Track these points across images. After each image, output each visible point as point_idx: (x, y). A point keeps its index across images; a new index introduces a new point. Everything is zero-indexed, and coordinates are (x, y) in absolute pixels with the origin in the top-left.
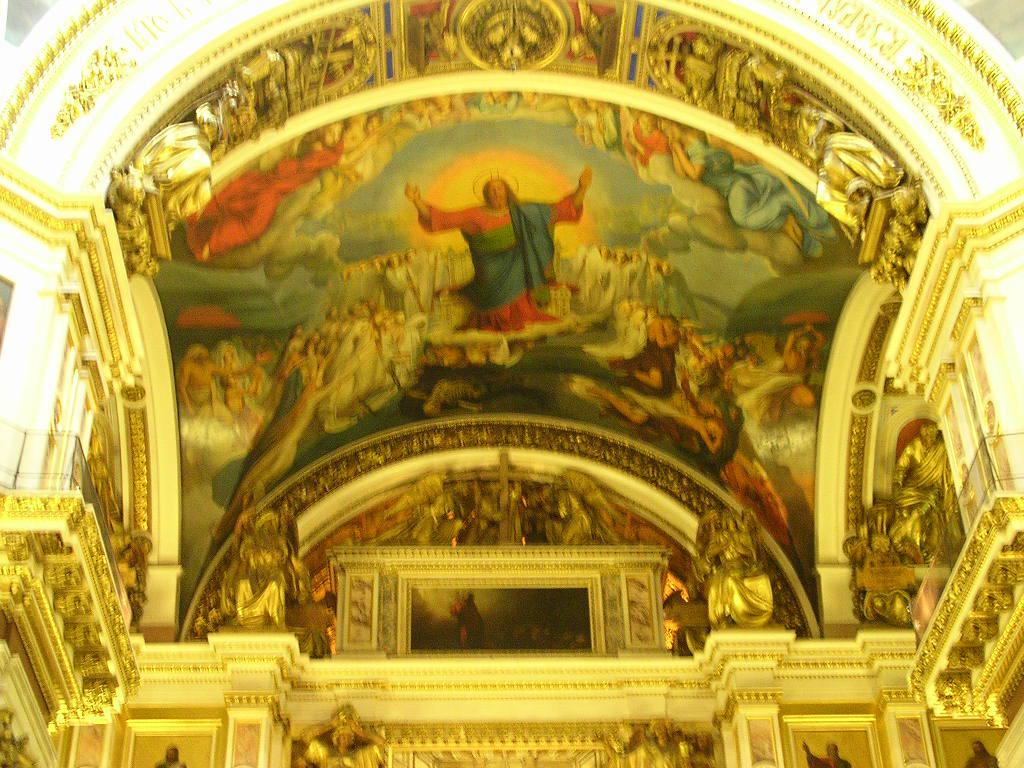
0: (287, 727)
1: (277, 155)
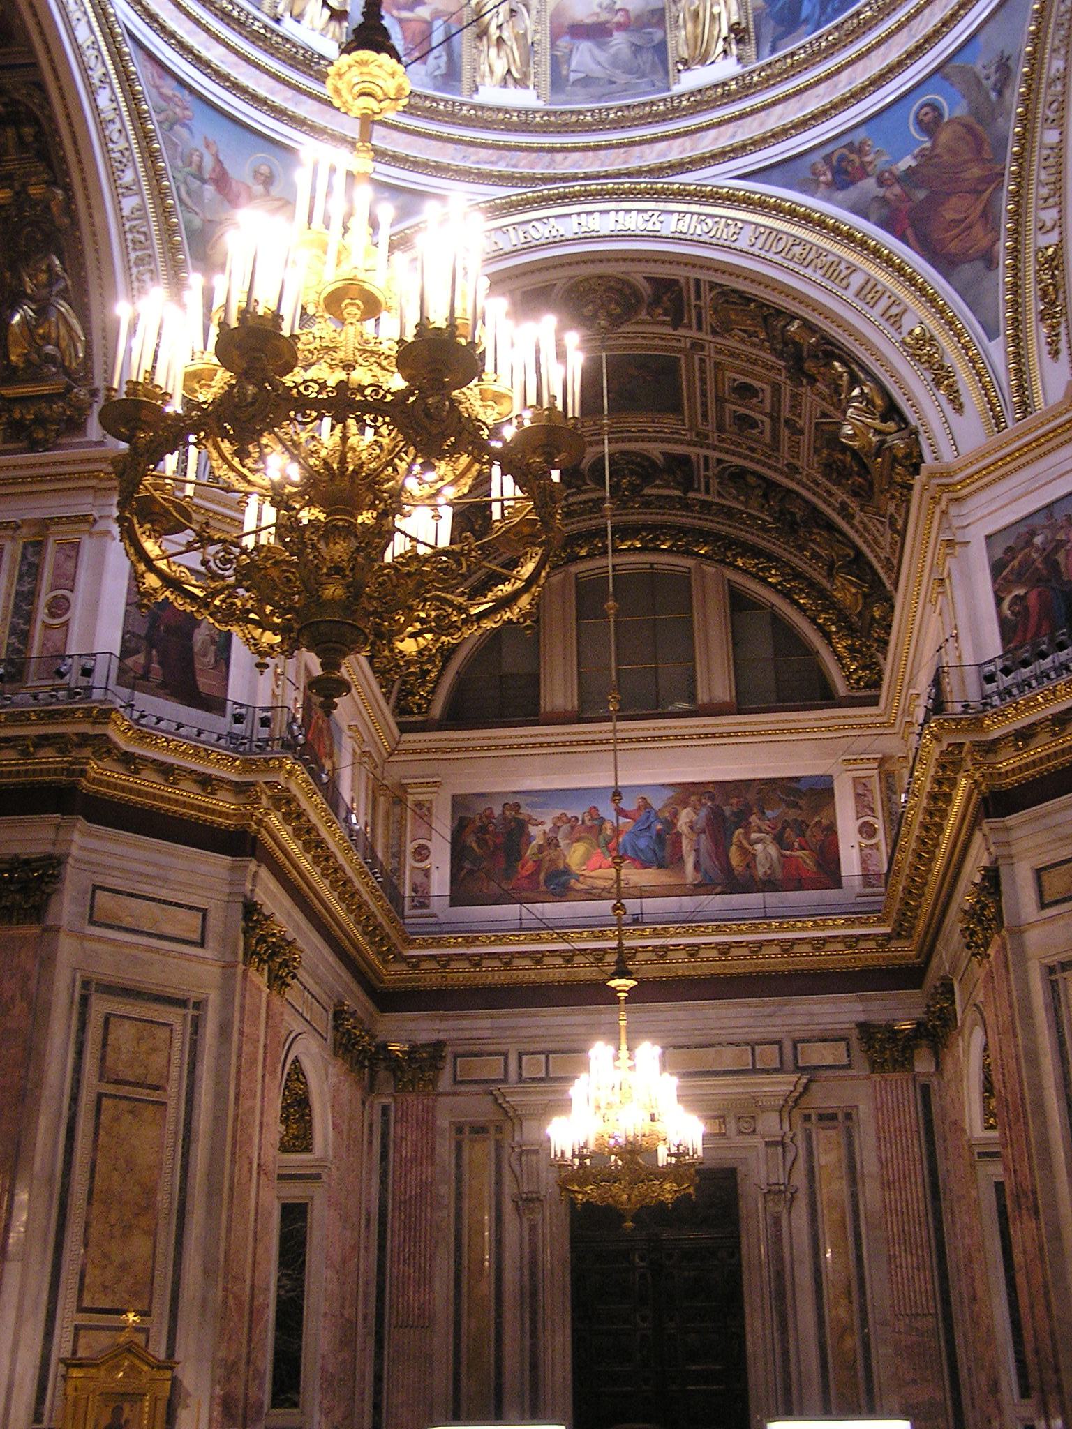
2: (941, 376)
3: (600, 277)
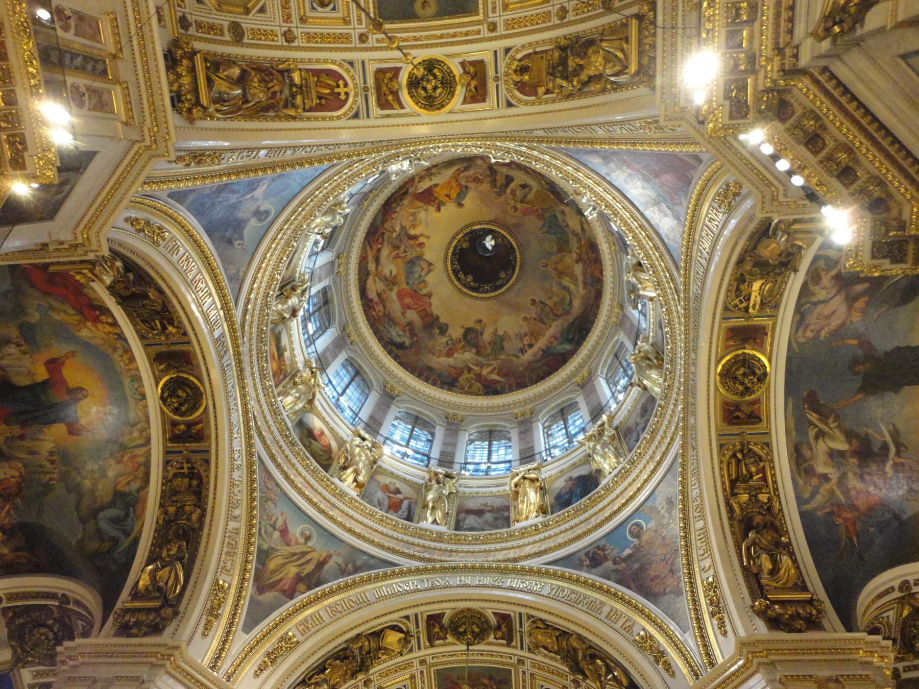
1: (91, 295)
2: (659, 656)
3: (469, 610)
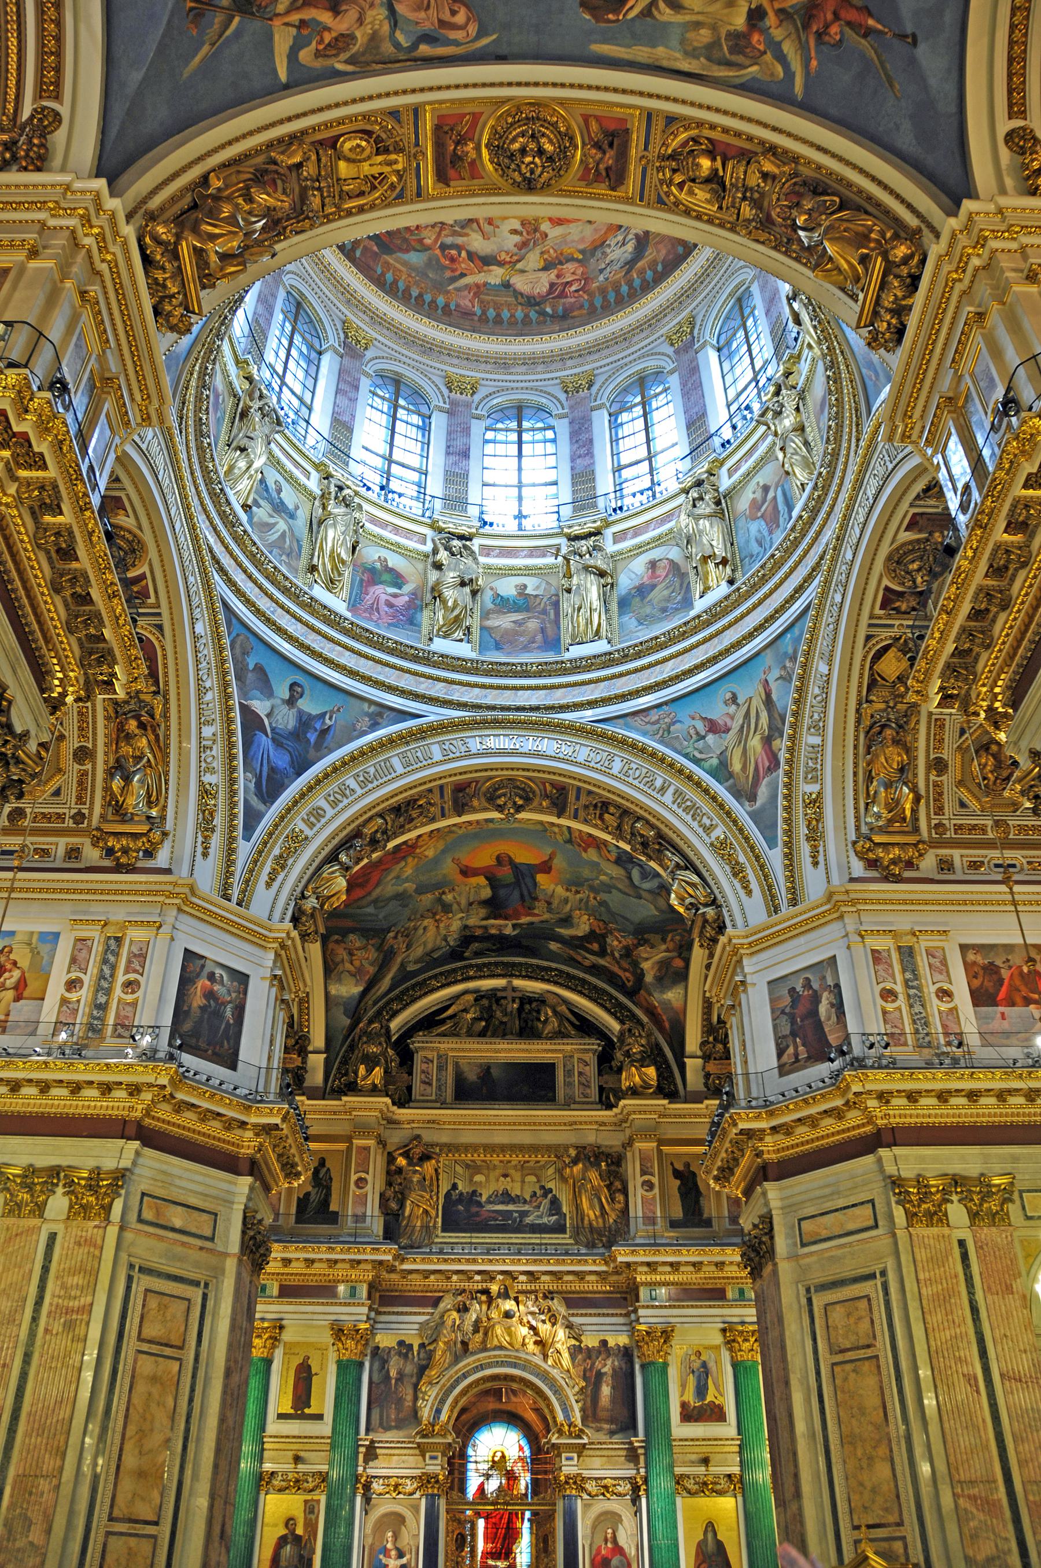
0: (385, 1146)
3: (889, 558)
